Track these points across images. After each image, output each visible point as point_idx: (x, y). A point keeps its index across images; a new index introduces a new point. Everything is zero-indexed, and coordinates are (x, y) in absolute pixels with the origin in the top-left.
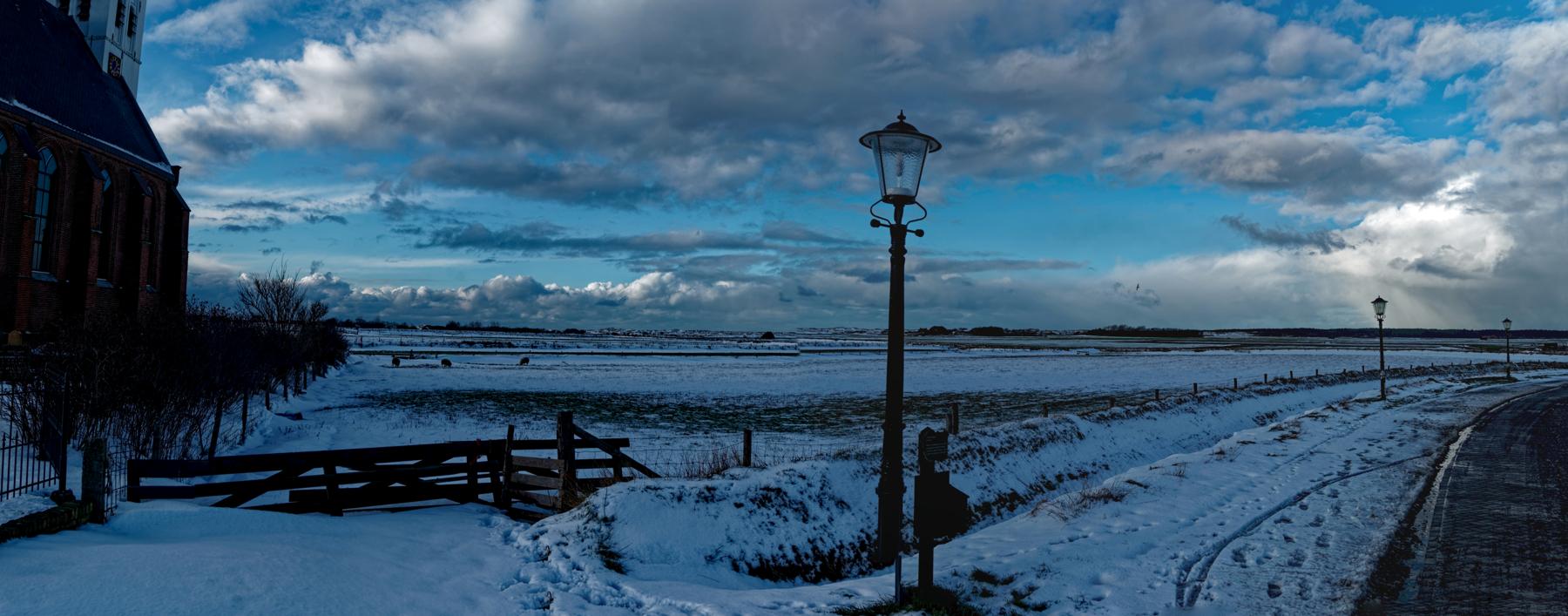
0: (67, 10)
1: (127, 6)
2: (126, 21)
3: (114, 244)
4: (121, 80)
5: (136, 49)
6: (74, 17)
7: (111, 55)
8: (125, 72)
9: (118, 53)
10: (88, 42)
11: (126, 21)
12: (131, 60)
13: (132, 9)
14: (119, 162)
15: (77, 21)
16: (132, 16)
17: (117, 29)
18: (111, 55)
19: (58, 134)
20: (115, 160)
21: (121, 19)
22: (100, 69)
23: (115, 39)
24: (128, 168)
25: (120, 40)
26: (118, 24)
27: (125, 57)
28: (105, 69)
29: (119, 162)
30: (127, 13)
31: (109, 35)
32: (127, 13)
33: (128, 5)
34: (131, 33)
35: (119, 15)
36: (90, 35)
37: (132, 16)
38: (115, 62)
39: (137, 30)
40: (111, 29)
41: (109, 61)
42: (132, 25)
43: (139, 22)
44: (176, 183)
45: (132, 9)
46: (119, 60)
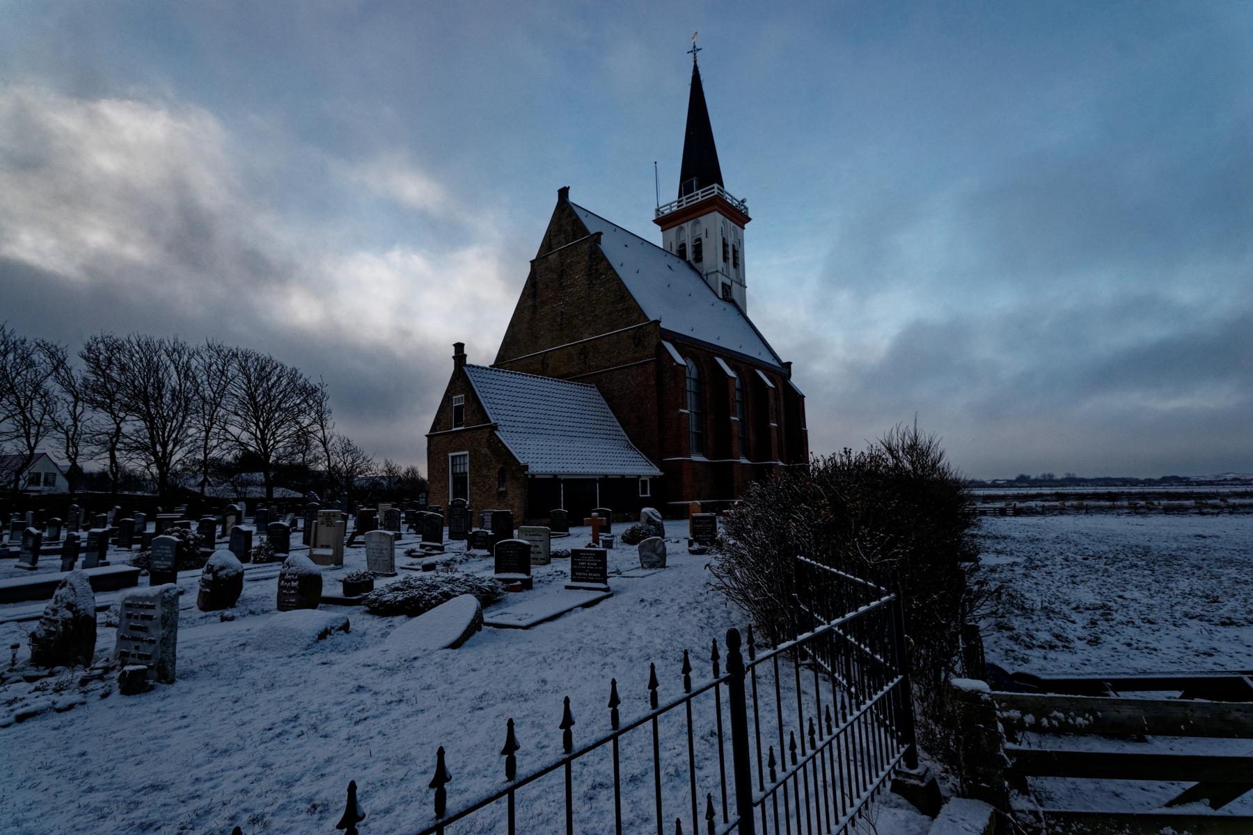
1: (729, 243)
2: (730, 255)
5: (741, 277)
7: (724, 284)
9: (728, 282)
11: (730, 255)
12: (739, 286)
16: (735, 252)
18: (724, 284)
26: (725, 259)
33: (730, 241)
34: (736, 265)
35: (725, 252)
36: (705, 273)
37: (735, 252)
41: (723, 289)
42: (735, 258)
45: (733, 246)
46: (730, 287)
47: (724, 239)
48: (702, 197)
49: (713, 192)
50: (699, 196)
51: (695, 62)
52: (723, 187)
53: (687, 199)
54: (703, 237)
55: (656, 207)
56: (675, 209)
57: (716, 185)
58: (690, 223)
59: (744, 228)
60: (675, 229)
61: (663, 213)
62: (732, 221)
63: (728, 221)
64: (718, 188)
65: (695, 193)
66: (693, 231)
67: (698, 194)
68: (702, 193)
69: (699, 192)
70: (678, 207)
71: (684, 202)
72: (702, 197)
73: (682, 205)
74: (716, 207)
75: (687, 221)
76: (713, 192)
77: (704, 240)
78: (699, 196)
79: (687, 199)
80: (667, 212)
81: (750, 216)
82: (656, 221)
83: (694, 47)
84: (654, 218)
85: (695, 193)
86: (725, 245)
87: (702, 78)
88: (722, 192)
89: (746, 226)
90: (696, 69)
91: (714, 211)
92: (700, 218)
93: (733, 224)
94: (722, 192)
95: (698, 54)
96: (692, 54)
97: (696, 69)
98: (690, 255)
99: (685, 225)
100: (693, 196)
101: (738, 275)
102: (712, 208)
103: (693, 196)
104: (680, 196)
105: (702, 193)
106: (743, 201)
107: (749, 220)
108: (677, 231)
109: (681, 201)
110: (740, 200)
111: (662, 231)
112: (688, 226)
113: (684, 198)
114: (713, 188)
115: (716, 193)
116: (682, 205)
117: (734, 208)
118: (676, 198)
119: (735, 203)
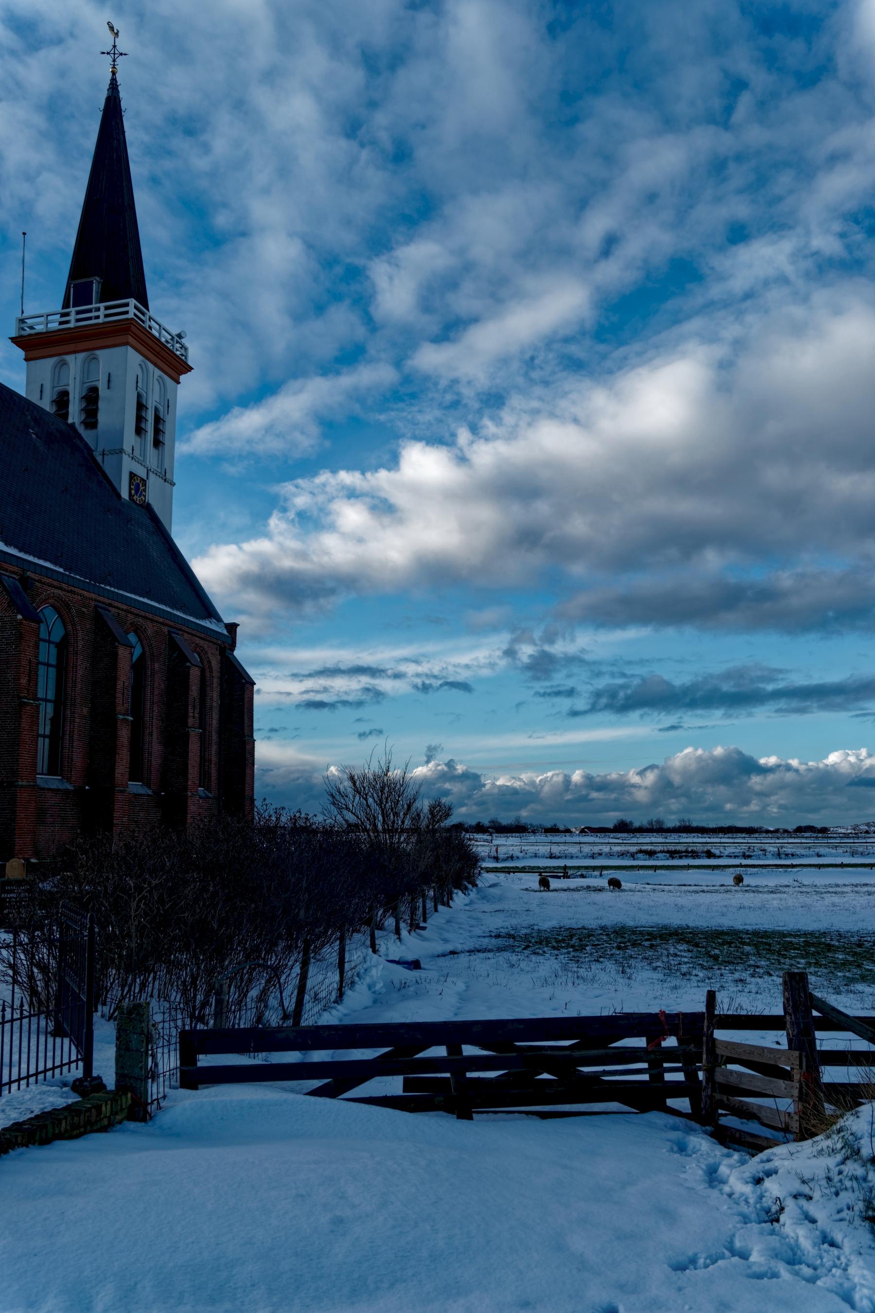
0: (66, 416)
1: (149, 406)
2: (150, 426)
3: (151, 734)
4: (148, 508)
5: (166, 465)
6: (77, 425)
7: (132, 475)
8: (153, 496)
9: (141, 472)
10: (99, 459)
11: (150, 426)
13: (156, 410)
14: (152, 620)
15: (81, 429)
16: (158, 420)
17: (138, 439)
18: (132, 475)
19: (64, 586)
20: (145, 618)
21: (143, 425)
22: (119, 496)
23: (137, 453)
24: (166, 629)
25: (143, 453)
27: (151, 475)
28: (125, 495)
29: (152, 620)
30: (150, 416)
31: (127, 448)
32: (150, 416)
33: (151, 405)
34: (157, 443)
35: (140, 419)
36: (100, 449)
37: (158, 420)
38: (138, 484)
39: (166, 439)
40: (130, 439)
41: (130, 483)
42: (157, 431)
43: (167, 428)
44: (233, 646)
45: (156, 410)
46: (144, 482)
47: (139, 396)
48: (106, 316)
49: (127, 313)
50: (101, 313)
51: (114, 73)
52: (147, 307)
53: (78, 313)
54: (102, 386)
55: (19, 316)
56: (54, 326)
57: (132, 302)
58: (81, 356)
59: (178, 382)
60: (51, 361)
61: (31, 328)
62: (155, 364)
63: (151, 366)
64: (136, 307)
65: (94, 306)
66: (86, 370)
67: (98, 309)
68: (107, 308)
69: (102, 306)
70: (61, 323)
71: (72, 317)
72: (106, 316)
73: (67, 322)
74: (131, 340)
75: (75, 352)
76: (127, 313)
77: (103, 392)
78: (101, 313)
79: (78, 313)
80: (40, 328)
81: (190, 363)
82: (18, 341)
83: (115, 46)
84: (13, 336)
85: (94, 306)
86: (141, 407)
87: (123, 105)
88: (143, 314)
89: (182, 378)
90: (114, 86)
91: (126, 344)
92: (98, 352)
93: (158, 372)
94: (143, 314)
95: (120, 60)
96: (109, 59)
97: (114, 86)
98: (75, 415)
99: (70, 358)
100: (90, 311)
101: (161, 461)
102: (122, 339)
103: (90, 311)
104: (66, 305)
105: (107, 308)
106: (180, 336)
107: (189, 369)
108: (55, 367)
109: (67, 314)
110: (175, 331)
111: (26, 359)
112: (75, 362)
113: (73, 310)
114: (127, 305)
115: (131, 315)
116: (67, 322)
117: (162, 346)
118: (58, 308)
119: (164, 337)
